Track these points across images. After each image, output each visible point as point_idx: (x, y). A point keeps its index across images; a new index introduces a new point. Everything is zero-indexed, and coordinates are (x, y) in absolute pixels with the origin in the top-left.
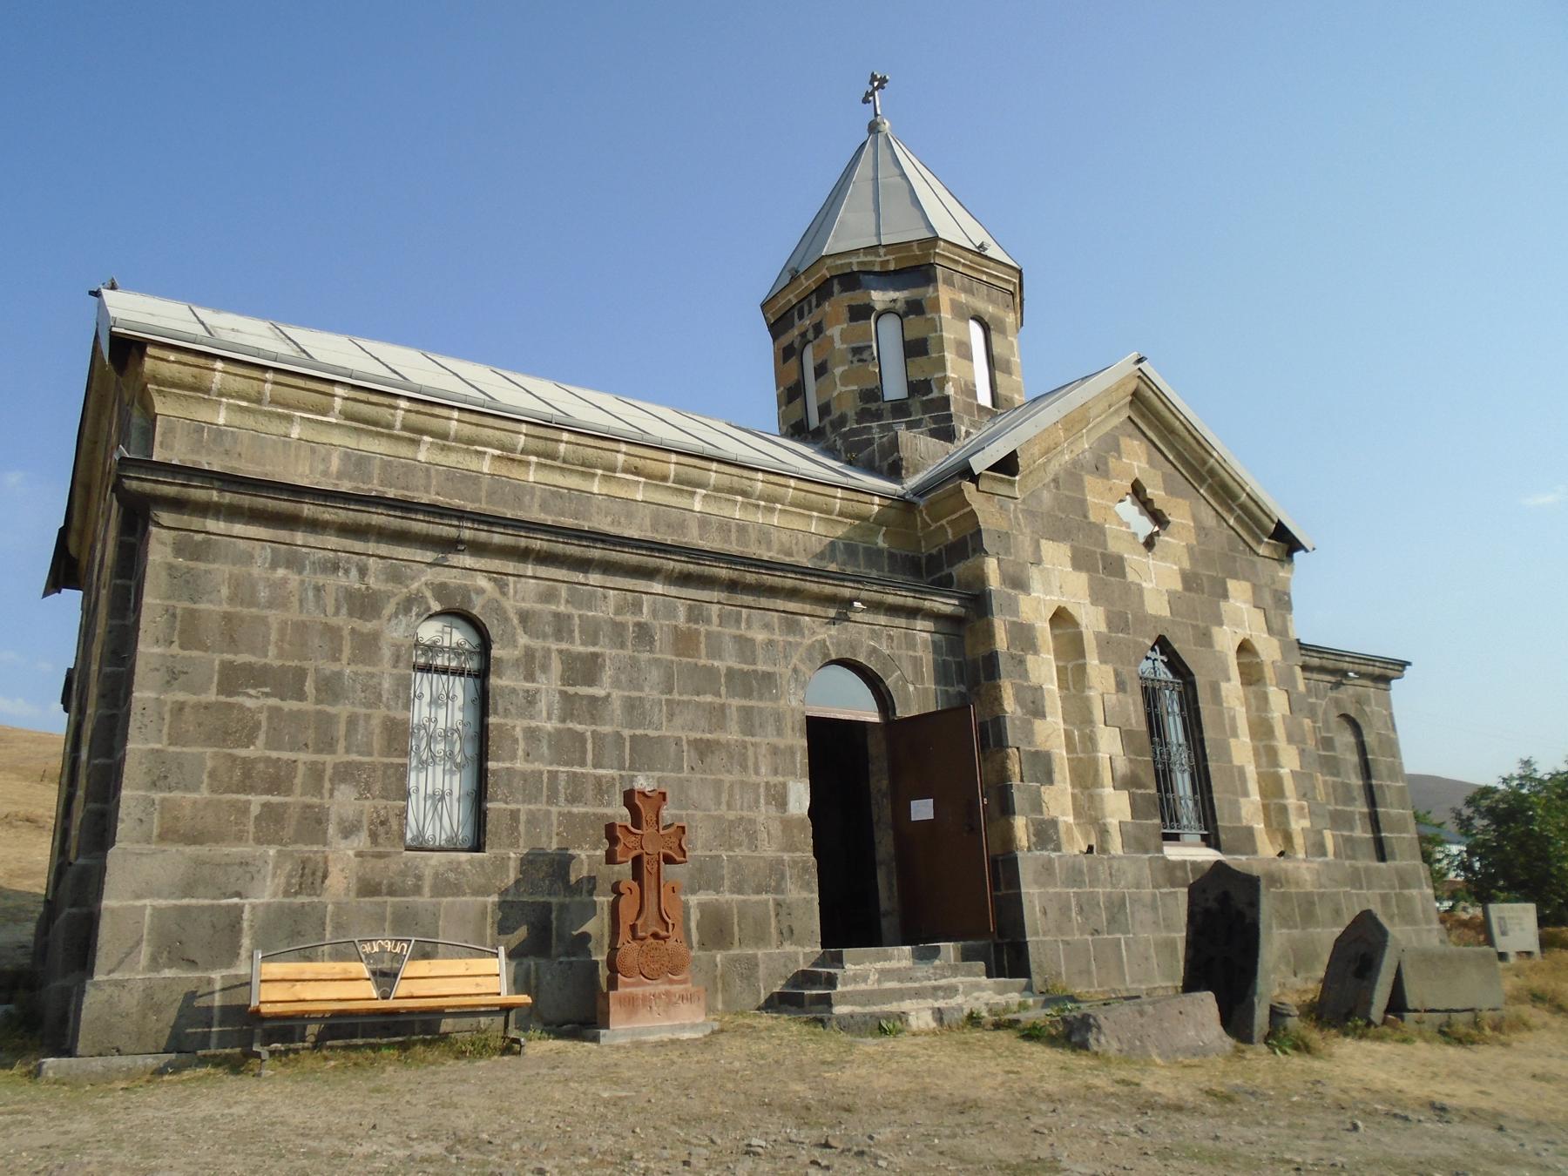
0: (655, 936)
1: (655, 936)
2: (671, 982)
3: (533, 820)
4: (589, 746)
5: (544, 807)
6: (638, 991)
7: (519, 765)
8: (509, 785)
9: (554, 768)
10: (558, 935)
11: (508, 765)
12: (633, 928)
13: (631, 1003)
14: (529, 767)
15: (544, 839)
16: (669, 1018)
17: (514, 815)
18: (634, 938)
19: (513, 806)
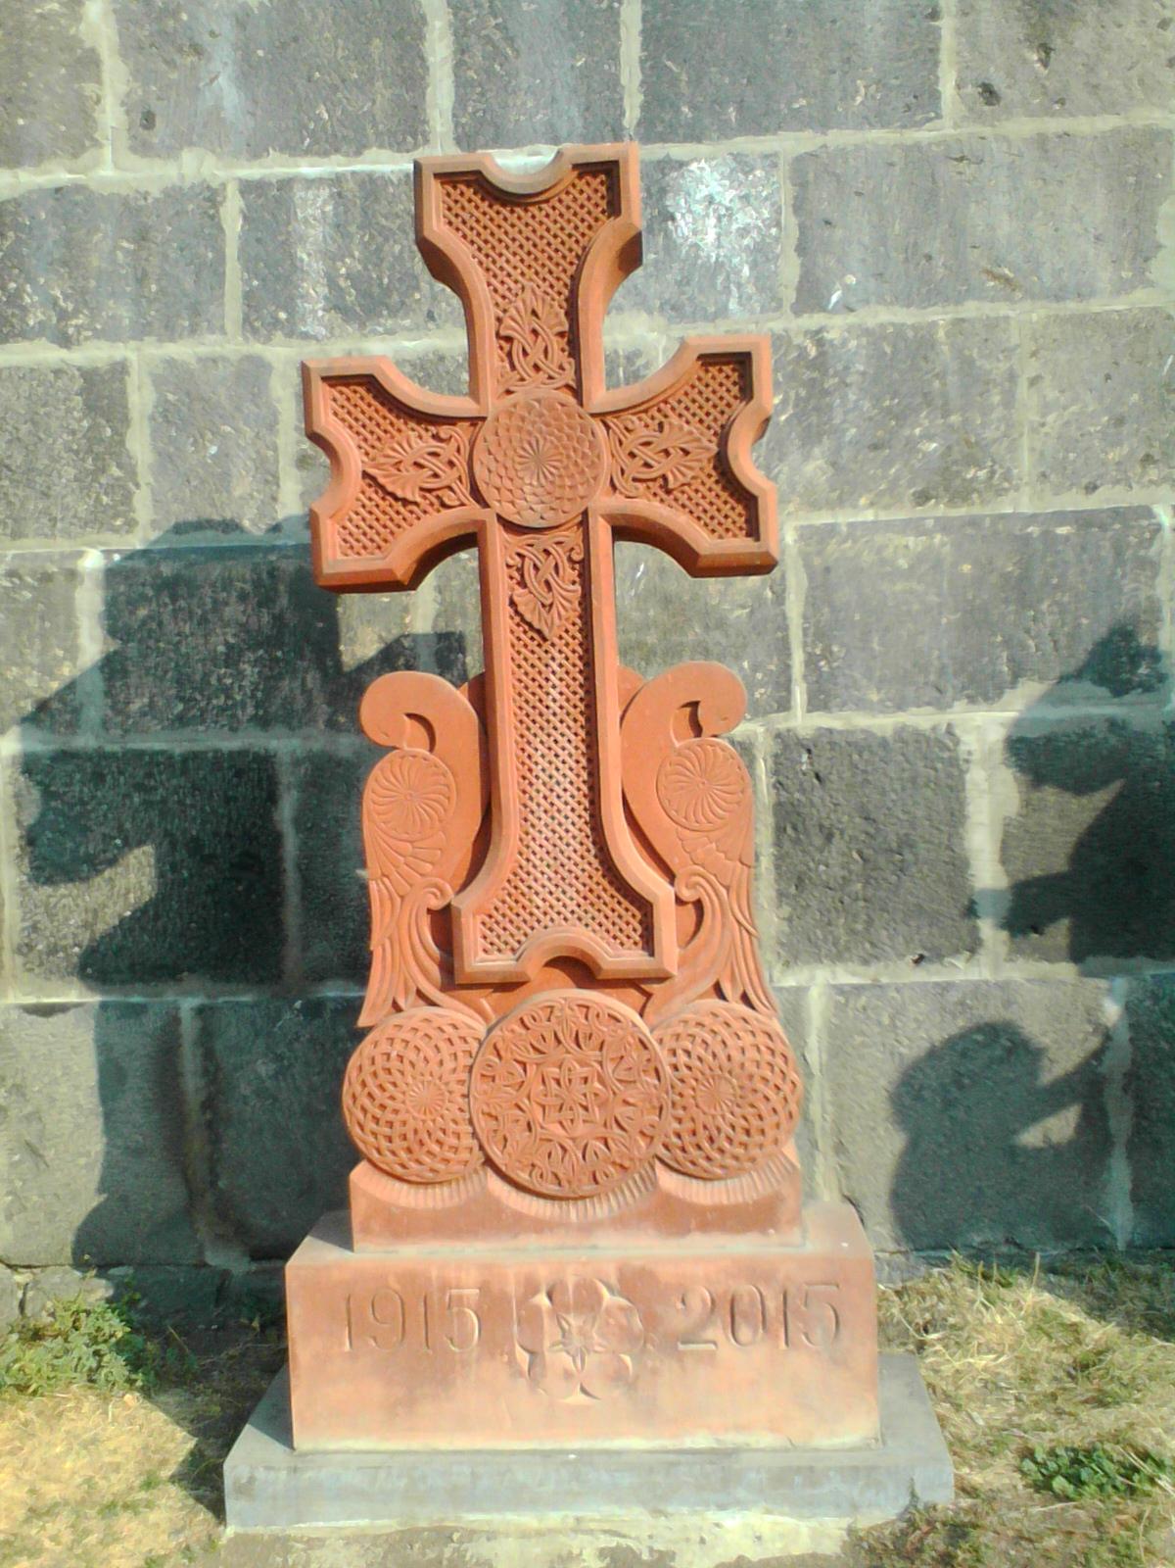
0: (579, 968)
1: (579, 968)
2: (675, 1218)
3: (186, 407)
4: (439, 48)
5: (230, 344)
6: (460, 1261)
7: (112, 169)
8: (71, 261)
9: (274, 167)
10: (307, 882)
11: (58, 174)
12: (444, 923)
13: (417, 1335)
14: (153, 175)
15: (243, 485)
16: (648, 1415)
17: (102, 393)
18: (452, 977)
19: (95, 353)
